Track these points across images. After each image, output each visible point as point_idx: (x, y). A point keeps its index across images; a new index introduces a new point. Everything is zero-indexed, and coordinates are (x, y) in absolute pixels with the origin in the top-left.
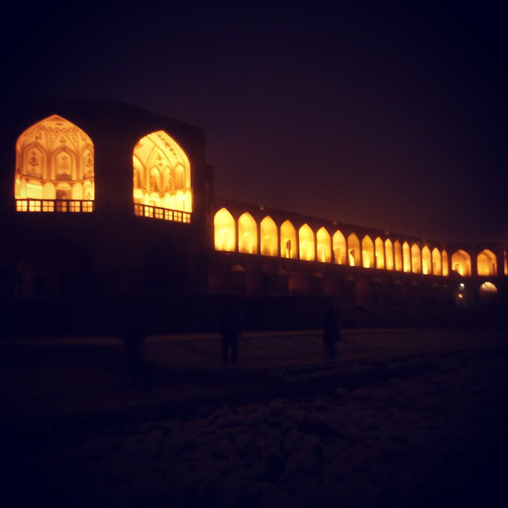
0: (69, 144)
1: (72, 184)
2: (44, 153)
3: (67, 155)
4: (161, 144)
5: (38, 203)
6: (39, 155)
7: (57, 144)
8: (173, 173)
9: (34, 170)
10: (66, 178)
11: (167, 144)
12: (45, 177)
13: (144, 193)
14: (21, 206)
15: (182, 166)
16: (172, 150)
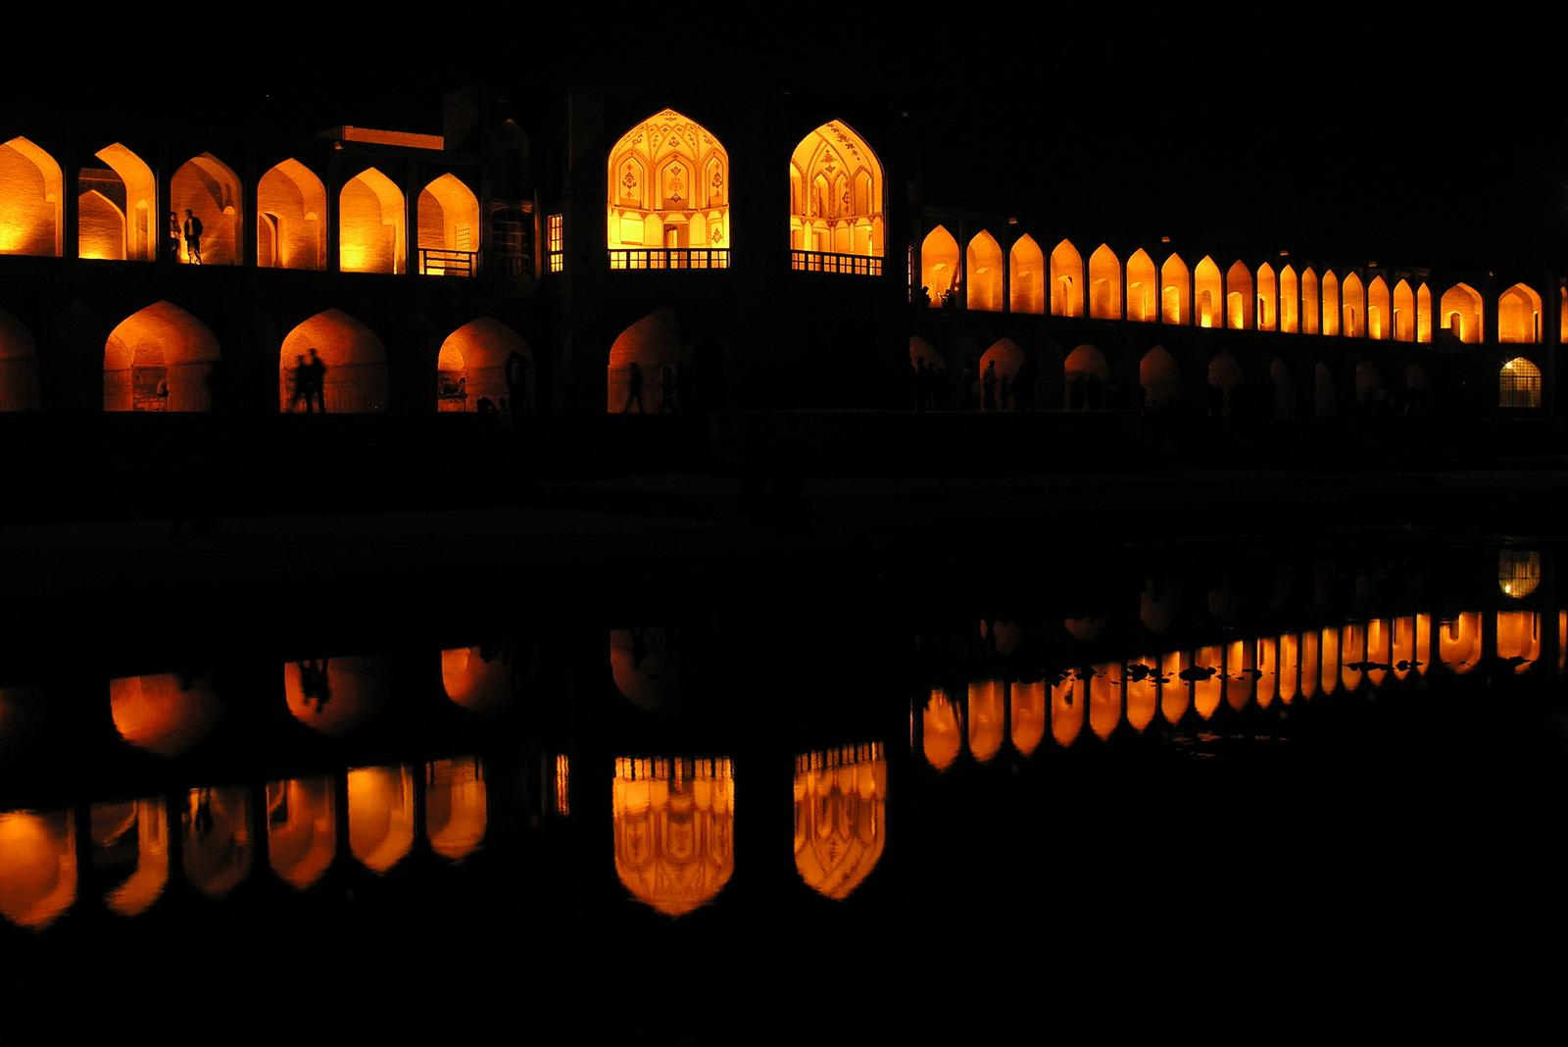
0: (683, 148)
1: (688, 217)
2: (643, 163)
3: (679, 166)
4: (832, 138)
5: (643, 255)
6: (637, 169)
7: (666, 149)
8: (851, 183)
9: (629, 194)
10: (675, 204)
11: (843, 137)
12: (646, 206)
13: (803, 223)
14: (618, 262)
15: (868, 173)
16: (850, 146)
